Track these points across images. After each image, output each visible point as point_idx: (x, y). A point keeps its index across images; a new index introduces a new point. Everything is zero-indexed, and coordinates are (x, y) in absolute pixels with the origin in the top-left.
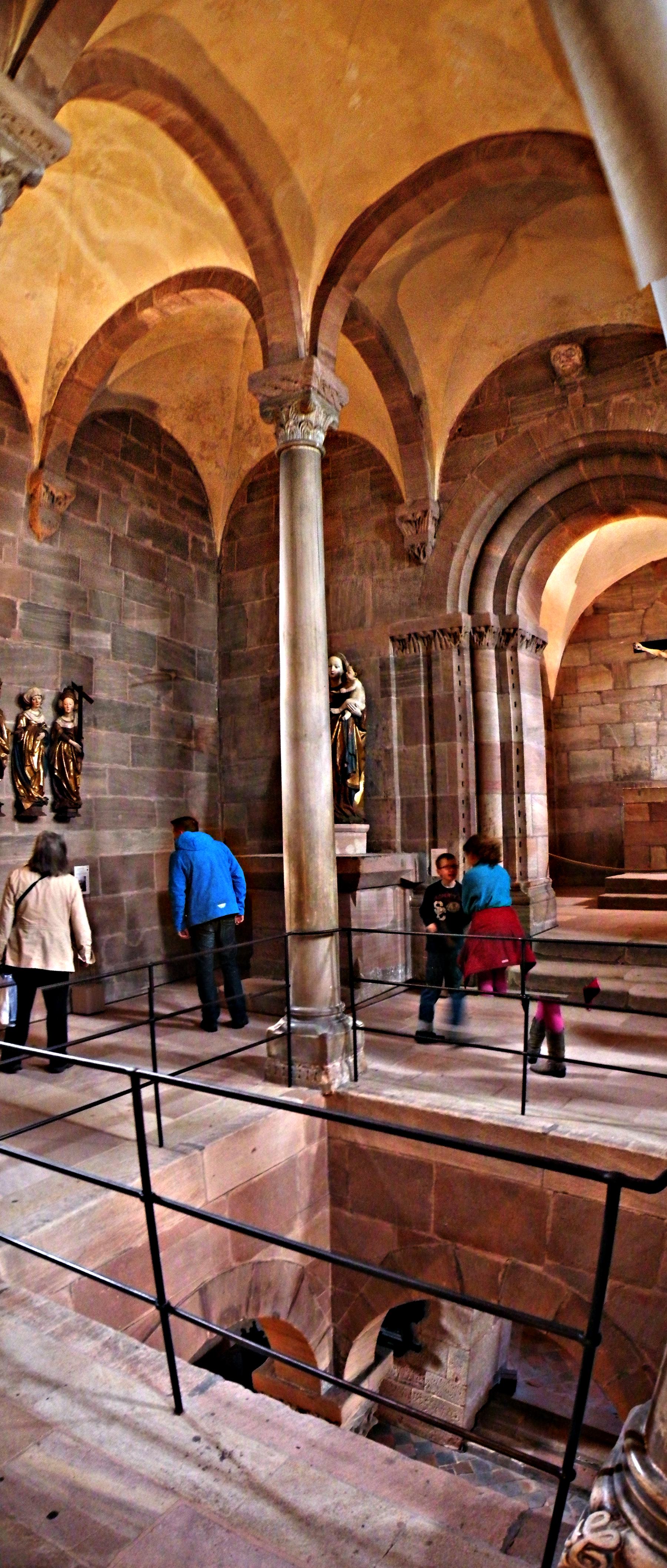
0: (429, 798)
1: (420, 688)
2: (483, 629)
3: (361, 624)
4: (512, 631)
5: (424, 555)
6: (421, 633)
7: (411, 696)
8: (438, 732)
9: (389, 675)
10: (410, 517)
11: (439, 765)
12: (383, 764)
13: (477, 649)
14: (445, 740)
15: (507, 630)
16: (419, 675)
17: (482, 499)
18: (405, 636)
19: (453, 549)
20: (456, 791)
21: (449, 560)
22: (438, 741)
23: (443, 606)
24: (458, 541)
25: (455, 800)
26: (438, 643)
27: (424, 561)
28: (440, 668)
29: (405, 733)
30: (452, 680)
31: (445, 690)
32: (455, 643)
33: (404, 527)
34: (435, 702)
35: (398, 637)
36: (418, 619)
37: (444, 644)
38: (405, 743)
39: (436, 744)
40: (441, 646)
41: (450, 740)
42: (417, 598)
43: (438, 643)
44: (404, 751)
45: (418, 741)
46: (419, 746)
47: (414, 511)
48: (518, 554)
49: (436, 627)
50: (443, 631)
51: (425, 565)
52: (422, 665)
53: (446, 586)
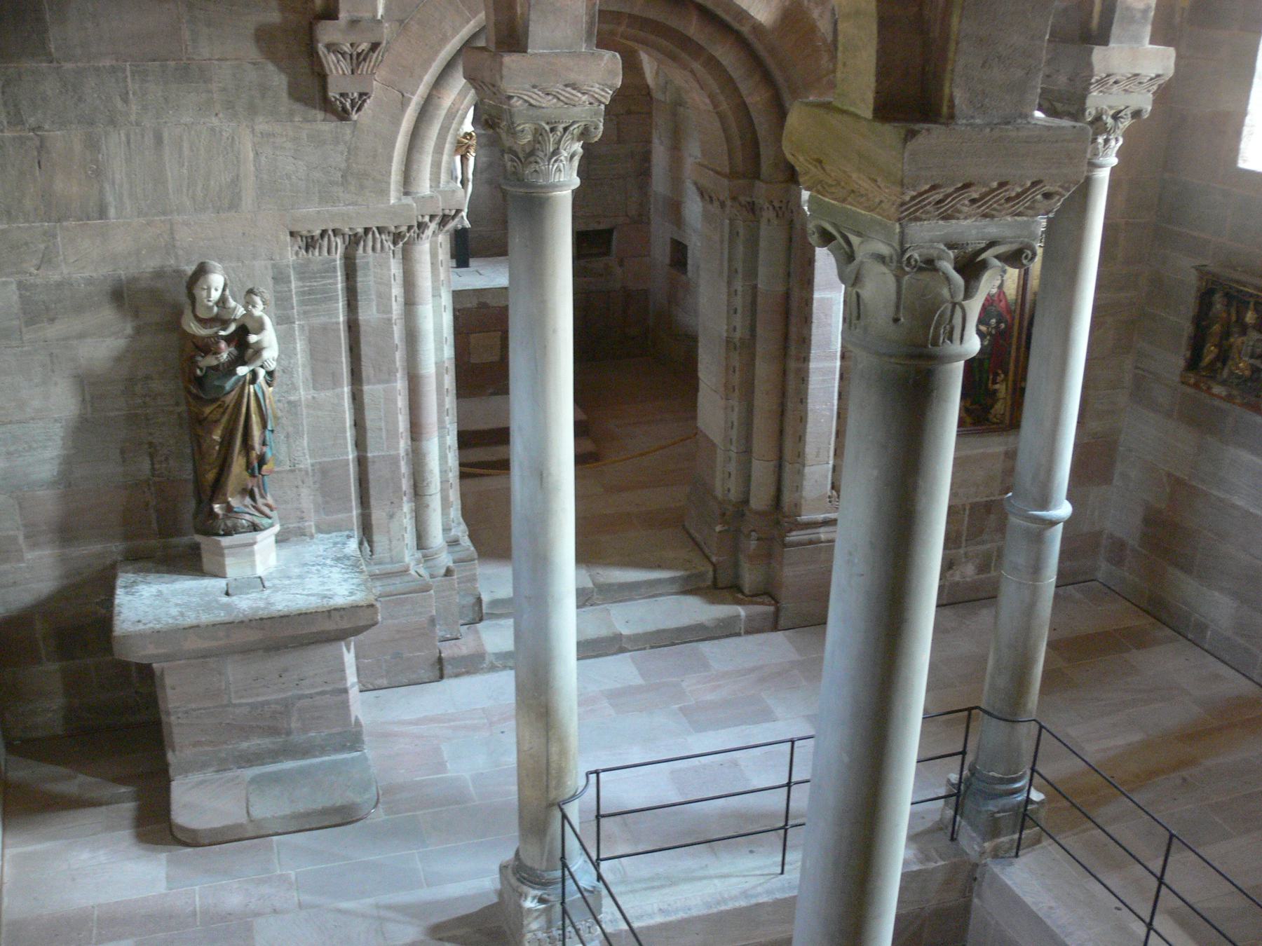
0: (353, 459)
1: (337, 309)
2: (427, 219)
3: (234, 205)
4: (453, 212)
5: (359, 109)
6: (346, 230)
7: (323, 319)
8: (367, 370)
9: (290, 291)
10: (346, 48)
11: (370, 416)
12: (284, 421)
13: (414, 244)
14: (380, 382)
15: (447, 212)
16: (336, 290)
17: (456, 31)
18: (317, 233)
19: (404, 104)
20: (397, 449)
21: (397, 122)
22: (369, 383)
23: (384, 192)
24: (413, 94)
25: (394, 461)
26: (370, 244)
27: (355, 116)
28: (372, 278)
29: (314, 373)
30: (390, 299)
31: (378, 311)
32: (395, 243)
33: (330, 60)
34: (363, 328)
35: (304, 233)
36: (341, 208)
37: (378, 246)
38: (315, 388)
39: (366, 388)
40: (374, 249)
41: (388, 381)
42: (339, 174)
43: (370, 244)
44: (314, 398)
45: (336, 383)
46: (338, 390)
47: (353, 38)
48: (465, 98)
49: (373, 224)
50: (381, 230)
51: (355, 121)
52: (339, 274)
53: (390, 160)
